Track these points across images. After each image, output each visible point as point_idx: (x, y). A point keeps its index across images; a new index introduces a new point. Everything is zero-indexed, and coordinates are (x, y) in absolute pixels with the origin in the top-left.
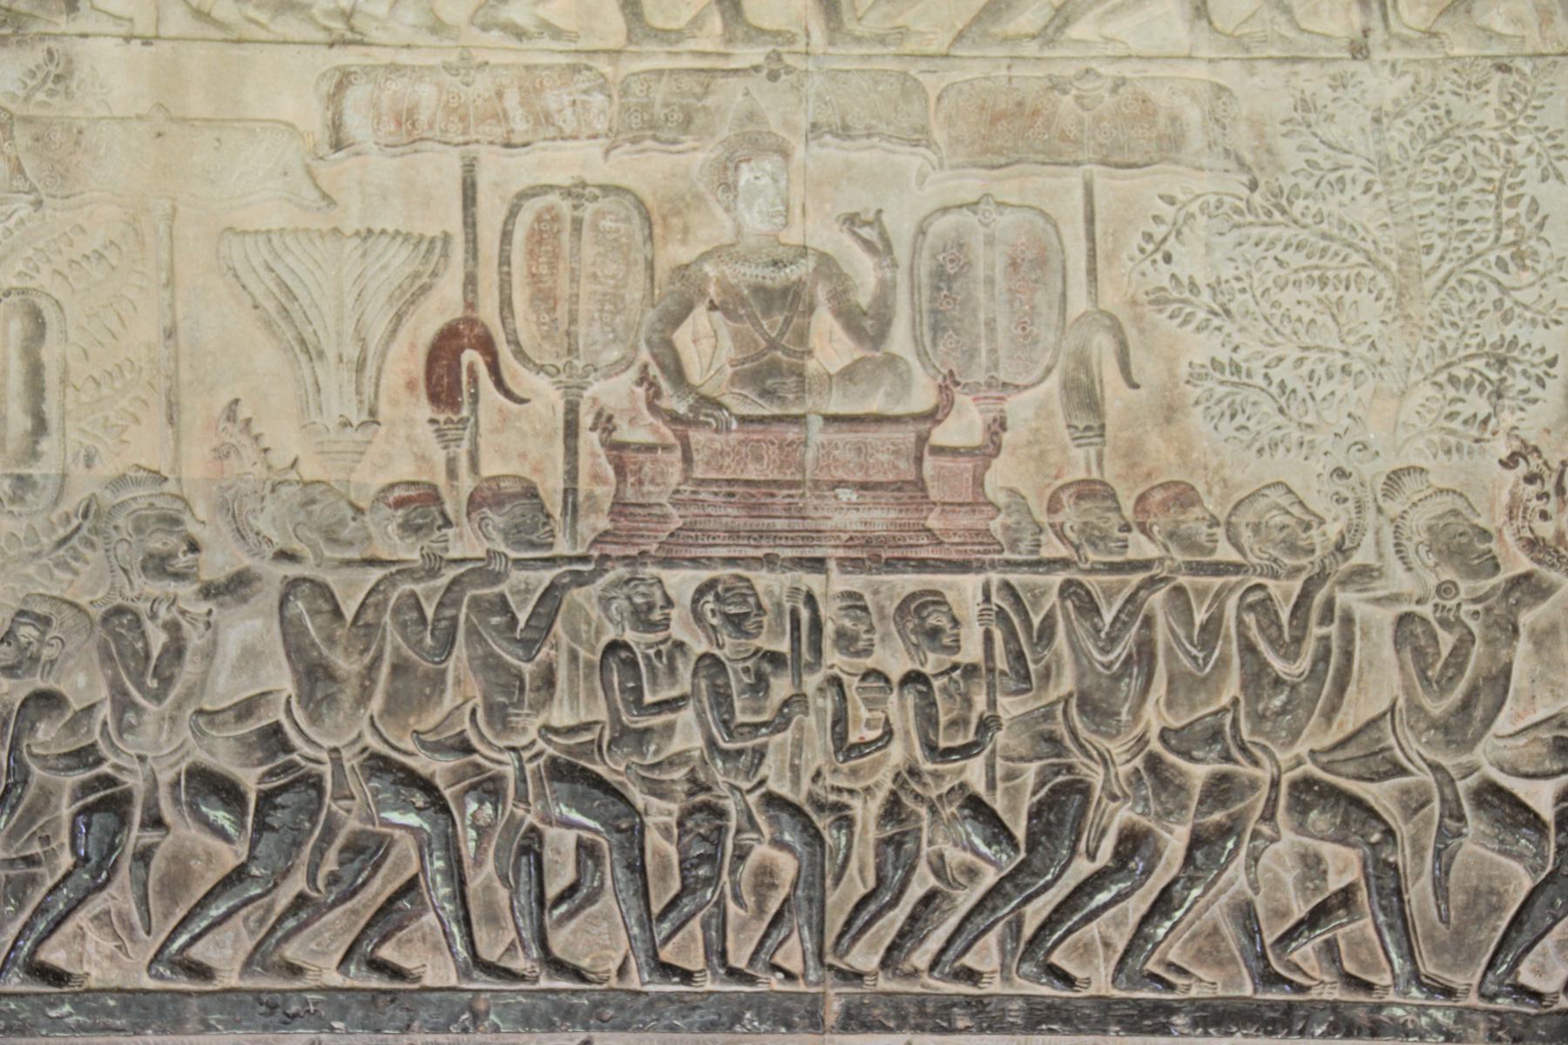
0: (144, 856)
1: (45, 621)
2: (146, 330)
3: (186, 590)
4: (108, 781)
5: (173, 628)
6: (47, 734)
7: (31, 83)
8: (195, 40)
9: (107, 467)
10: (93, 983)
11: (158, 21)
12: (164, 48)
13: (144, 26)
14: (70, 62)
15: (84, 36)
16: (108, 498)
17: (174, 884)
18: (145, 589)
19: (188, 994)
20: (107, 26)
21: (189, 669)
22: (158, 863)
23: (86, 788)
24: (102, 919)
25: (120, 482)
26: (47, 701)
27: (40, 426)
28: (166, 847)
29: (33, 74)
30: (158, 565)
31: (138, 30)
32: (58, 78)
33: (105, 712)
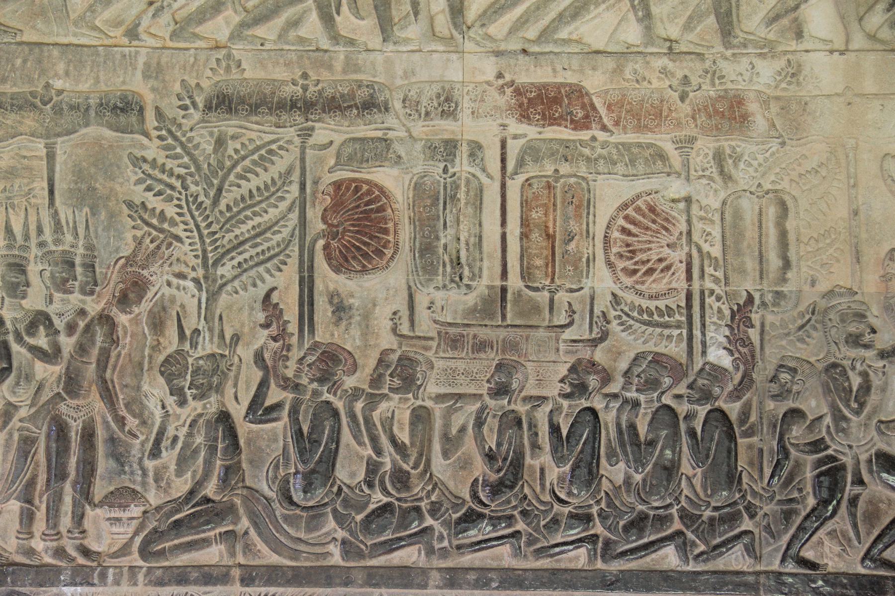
0: (854, 501)
1: (794, 371)
2: (842, 211)
3: (869, 354)
4: (832, 459)
5: (865, 375)
6: (796, 432)
7: (778, 78)
8: (868, 51)
9: (823, 286)
10: (830, 569)
11: (847, 42)
12: (851, 56)
13: (839, 44)
14: (800, 66)
15: (807, 51)
16: (823, 304)
17: (872, 516)
18: (846, 354)
19: (886, 577)
20: (821, 46)
21: (873, 398)
22: (861, 505)
23: (819, 463)
24: (832, 534)
25: (830, 294)
26: (795, 414)
27: (787, 264)
28: (865, 495)
29: (779, 74)
30: (855, 340)
31: (836, 47)
32: (793, 75)
33: (828, 420)
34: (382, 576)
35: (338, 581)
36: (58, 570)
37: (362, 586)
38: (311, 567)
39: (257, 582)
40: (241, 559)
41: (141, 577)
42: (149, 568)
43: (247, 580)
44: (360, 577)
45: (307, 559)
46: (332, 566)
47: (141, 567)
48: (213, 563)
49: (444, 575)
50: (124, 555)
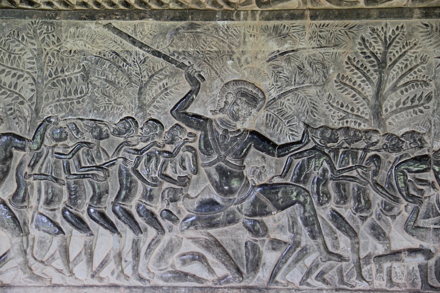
34: (387, 13)
35: (363, 16)
36: (214, 12)
37: (376, 19)
38: (349, 9)
39: (319, 18)
40: (310, 6)
41: (258, 16)
42: (262, 11)
43: (313, 17)
44: (375, 13)
45: (346, 5)
46: (359, 8)
47: (257, 11)
48: (295, 8)
49: (422, 11)
50: (248, 4)
